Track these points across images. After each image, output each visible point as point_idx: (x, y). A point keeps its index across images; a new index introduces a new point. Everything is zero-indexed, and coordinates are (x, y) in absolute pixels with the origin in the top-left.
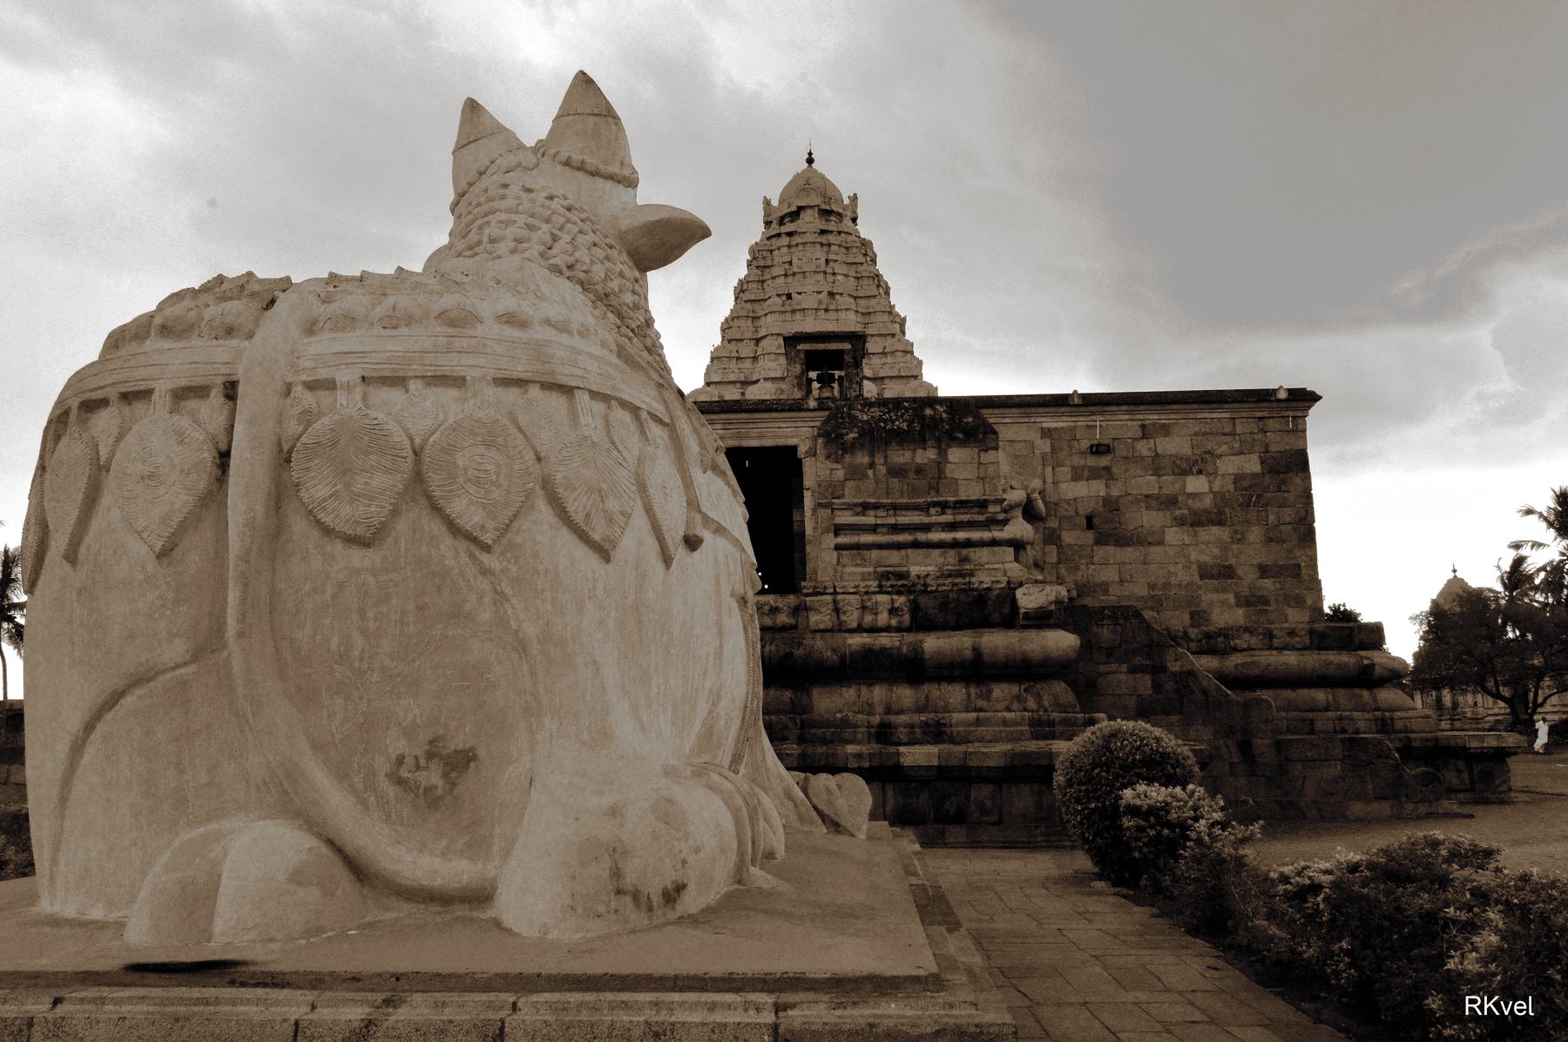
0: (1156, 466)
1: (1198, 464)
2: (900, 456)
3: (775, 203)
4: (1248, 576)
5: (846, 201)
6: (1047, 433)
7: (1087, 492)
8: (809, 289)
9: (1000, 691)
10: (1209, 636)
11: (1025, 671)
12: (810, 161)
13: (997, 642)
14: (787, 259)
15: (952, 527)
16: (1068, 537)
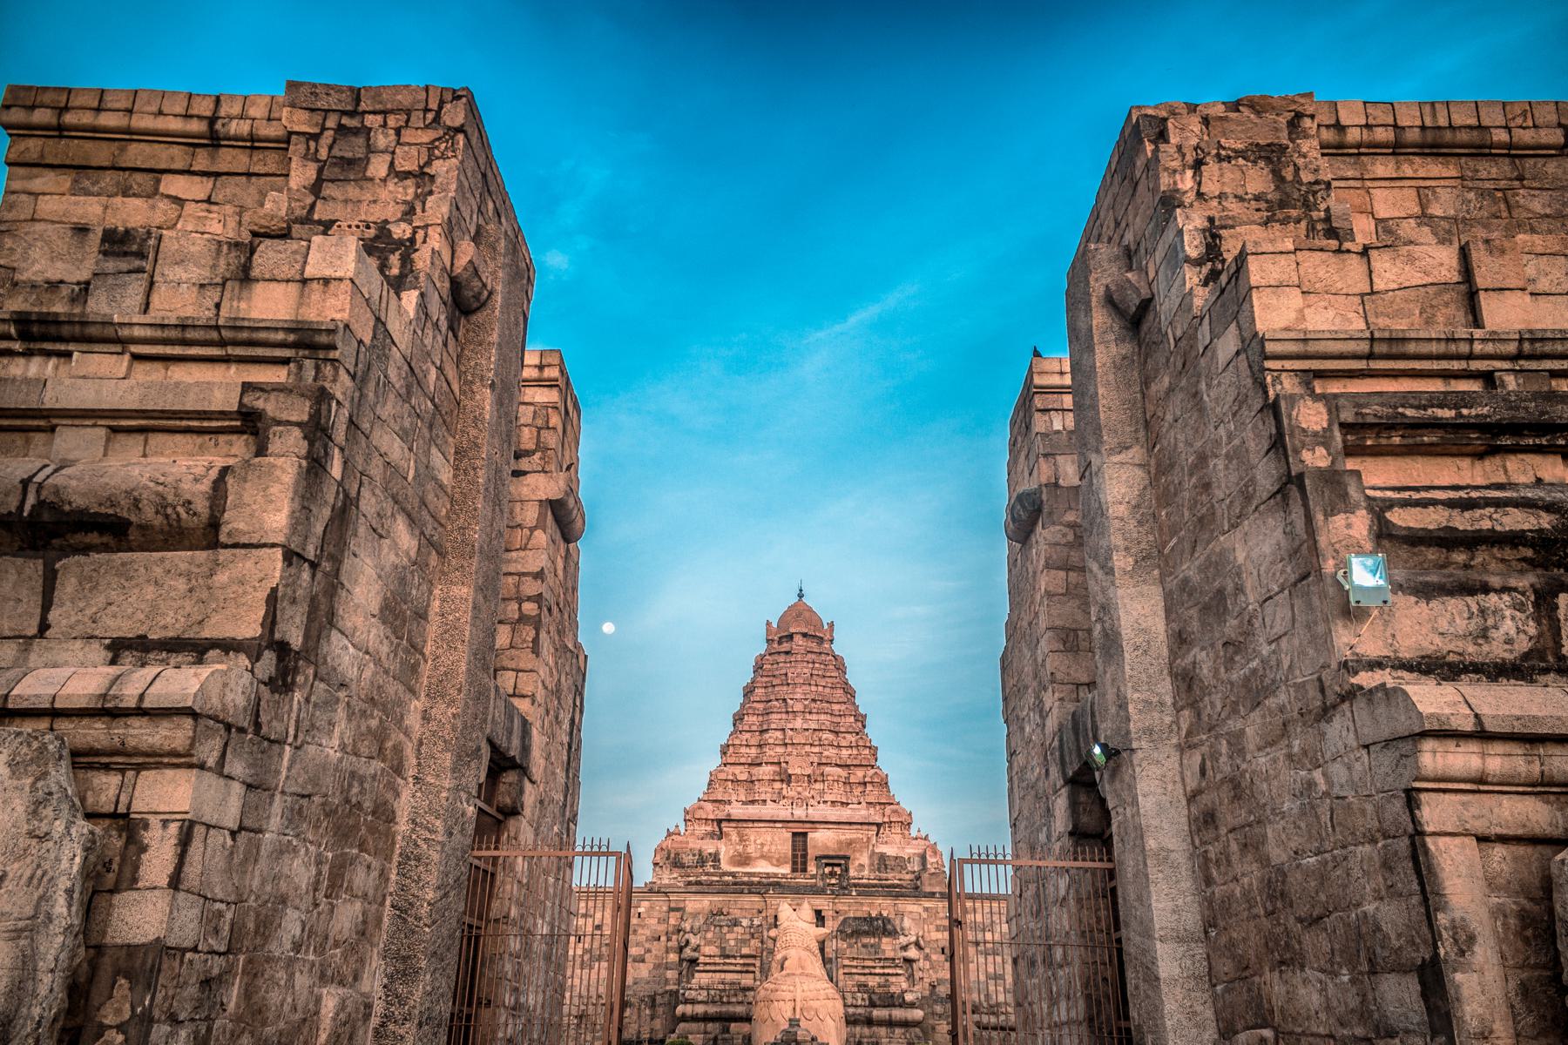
2: (866, 940)
9: (898, 1031)
11: (906, 1024)
13: (898, 1013)
16: (934, 957)
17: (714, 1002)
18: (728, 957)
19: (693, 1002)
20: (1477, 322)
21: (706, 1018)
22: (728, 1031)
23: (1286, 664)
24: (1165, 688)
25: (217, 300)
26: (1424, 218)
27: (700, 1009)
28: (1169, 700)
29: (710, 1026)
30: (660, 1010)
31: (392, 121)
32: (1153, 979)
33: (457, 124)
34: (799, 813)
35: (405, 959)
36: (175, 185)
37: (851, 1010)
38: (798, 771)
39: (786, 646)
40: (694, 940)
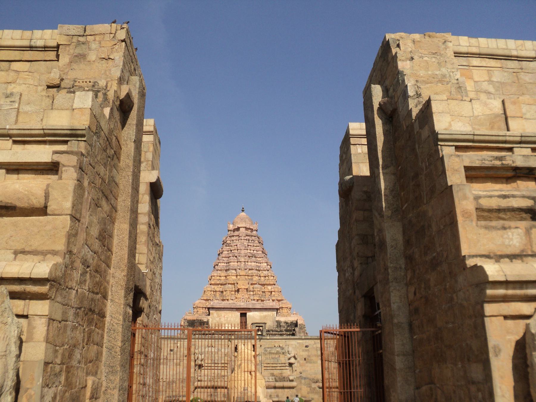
7: (305, 354)
14: (235, 244)
16: (301, 362)
20: (508, 130)
21: (206, 387)
23: (445, 256)
24: (402, 262)
25: (41, 118)
26: (490, 81)
28: (403, 266)
29: (209, 390)
31: (98, 38)
32: (393, 369)
33: (122, 39)
34: (243, 305)
35: (112, 367)
36: (16, 66)
38: (243, 287)
39: (236, 233)
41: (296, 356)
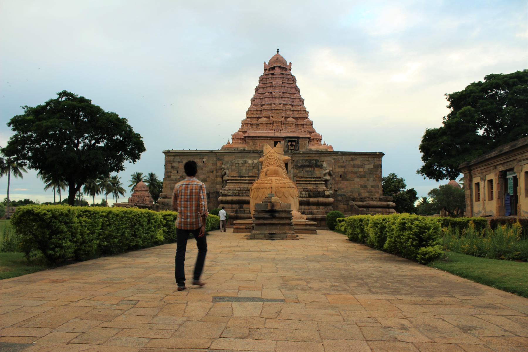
0: (354, 166)
1: (362, 166)
2: (308, 169)
3: (267, 64)
4: (369, 187)
5: (288, 64)
6: (334, 159)
8: (277, 91)
9: (321, 207)
10: (361, 198)
11: (325, 204)
12: (278, 52)
13: (321, 200)
14: (271, 81)
15: (315, 181)
16: (337, 179)
17: (236, 196)
18: (242, 177)
19: (226, 195)
21: (232, 202)
22: (242, 208)
27: (229, 198)
29: (234, 206)
30: (212, 199)
34: (277, 135)
37: (300, 199)
39: (272, 72)
40: (227, 172)
41: (332, 173)
